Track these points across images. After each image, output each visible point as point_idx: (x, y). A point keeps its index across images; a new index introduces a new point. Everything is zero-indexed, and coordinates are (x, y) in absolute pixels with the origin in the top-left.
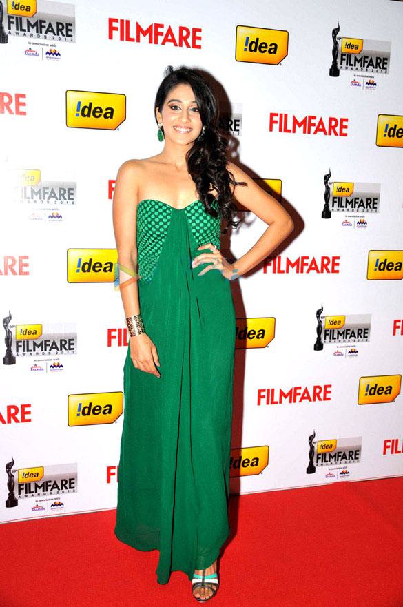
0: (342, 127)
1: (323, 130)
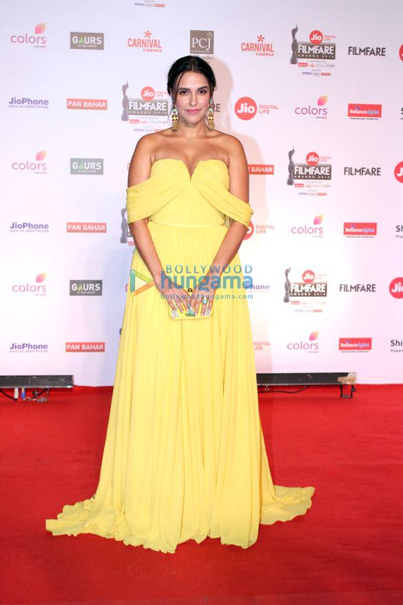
0: (383, 52)
1: (374, 53)
